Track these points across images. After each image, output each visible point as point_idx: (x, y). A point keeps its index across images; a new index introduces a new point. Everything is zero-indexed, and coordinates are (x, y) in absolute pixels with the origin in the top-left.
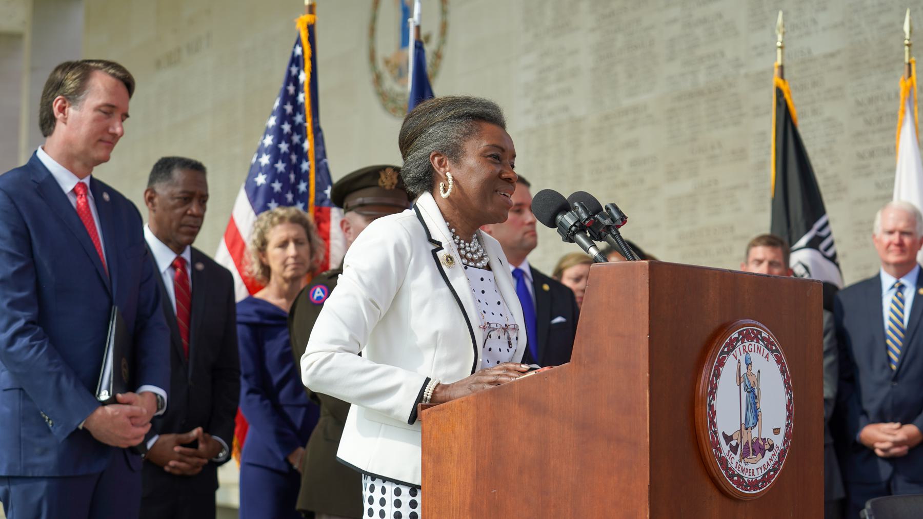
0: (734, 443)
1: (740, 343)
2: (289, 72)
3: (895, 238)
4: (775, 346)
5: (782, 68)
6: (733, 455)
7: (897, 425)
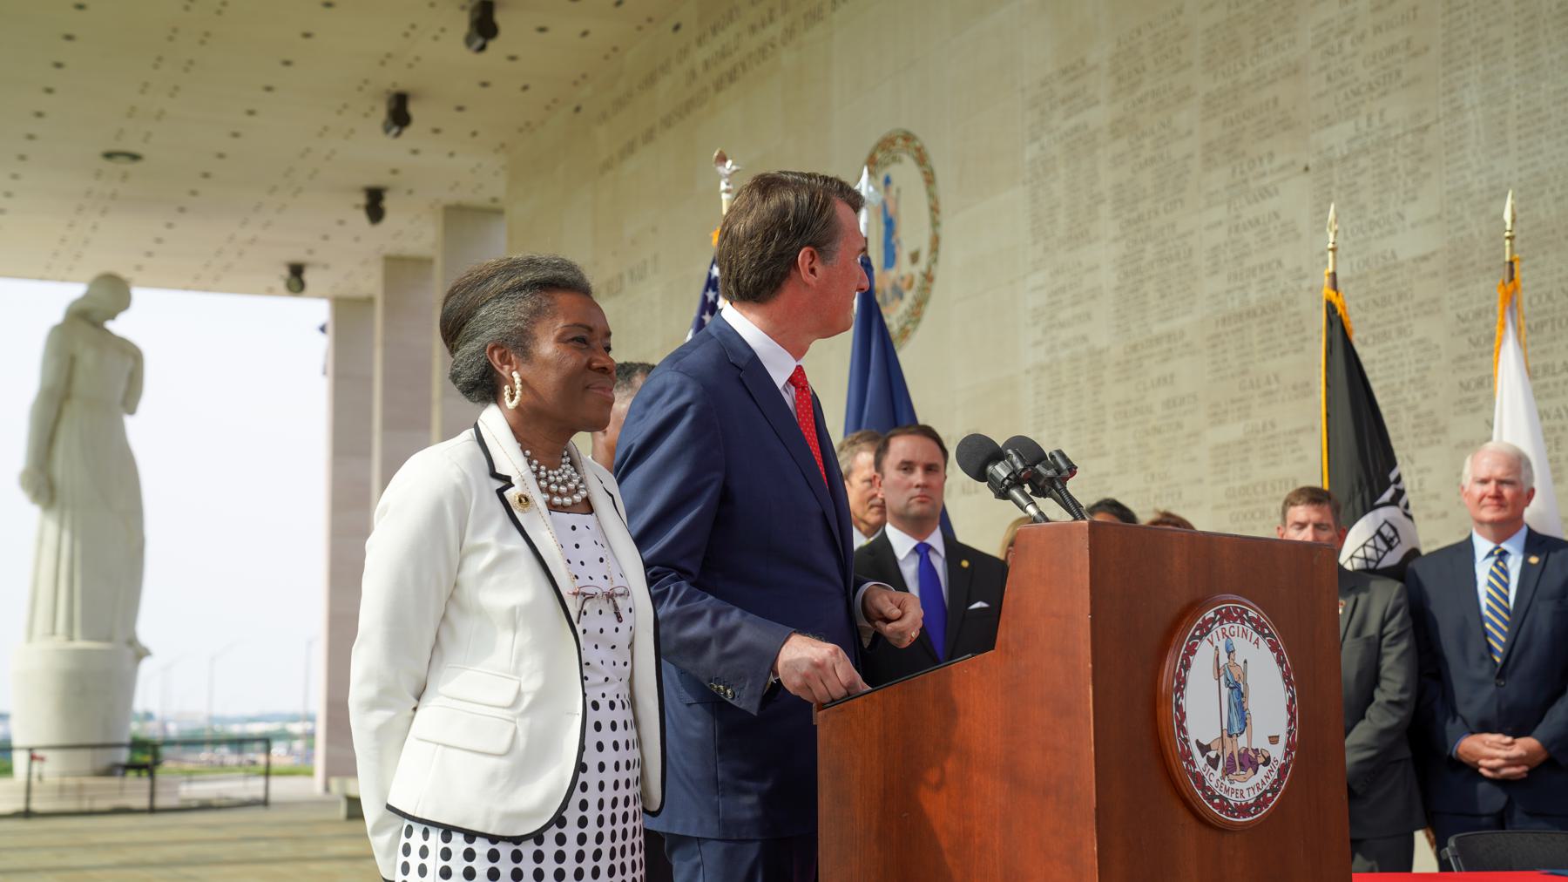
0: (1212, 754)
1: (1217, 624)
2: (705, 298)
3: (1490, 488)
4: (1268, 628)
5: (1334, 275)
6: (1212, 770)
7: (1509, 739)
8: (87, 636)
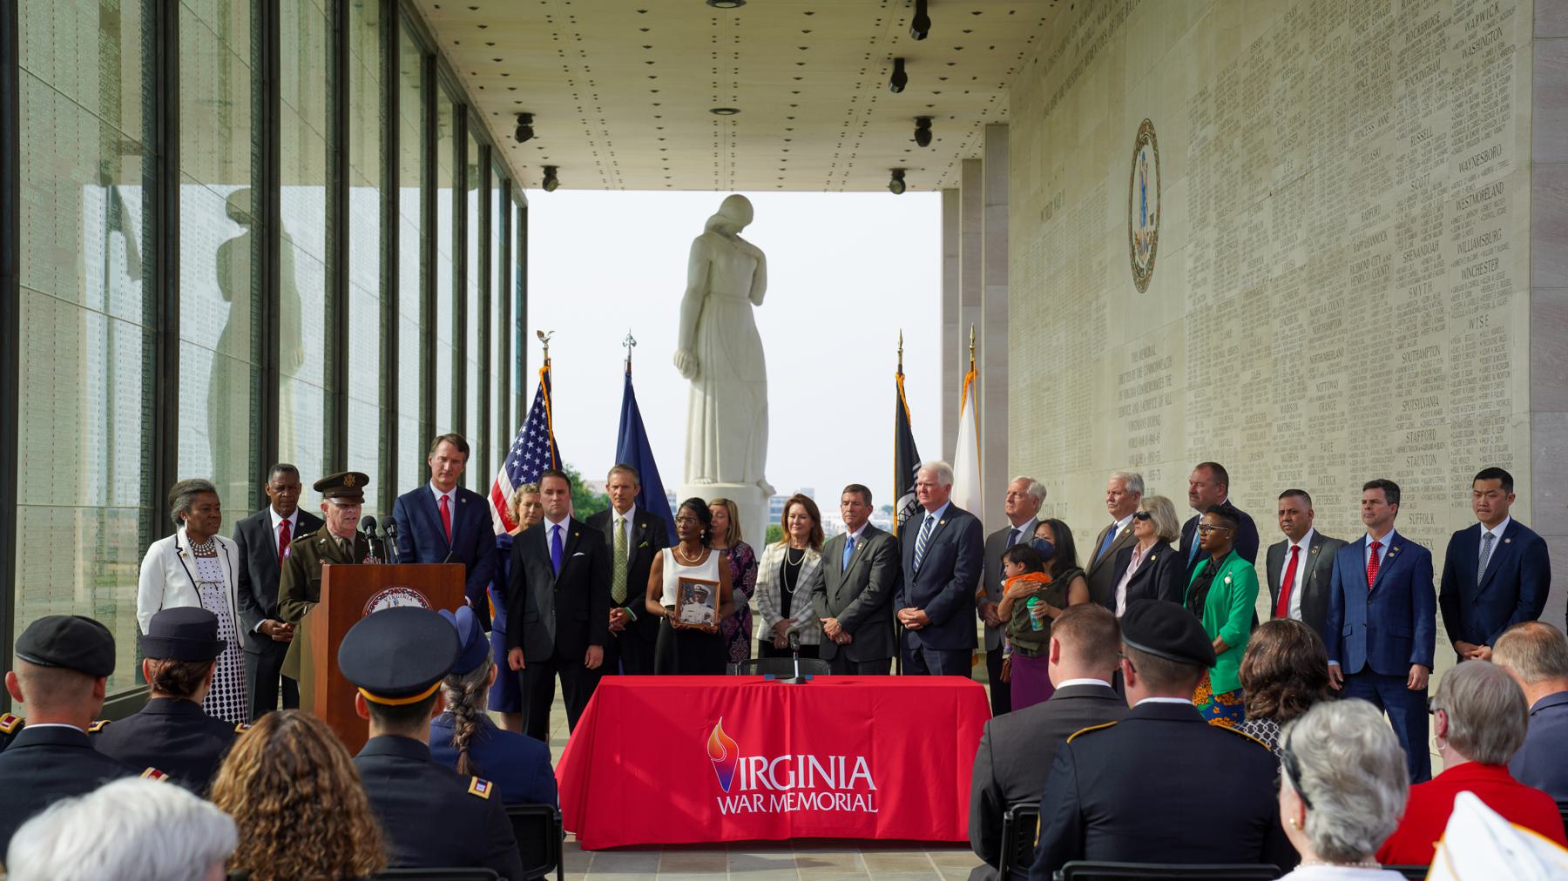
2: (536, 400)
8: (724, 481)
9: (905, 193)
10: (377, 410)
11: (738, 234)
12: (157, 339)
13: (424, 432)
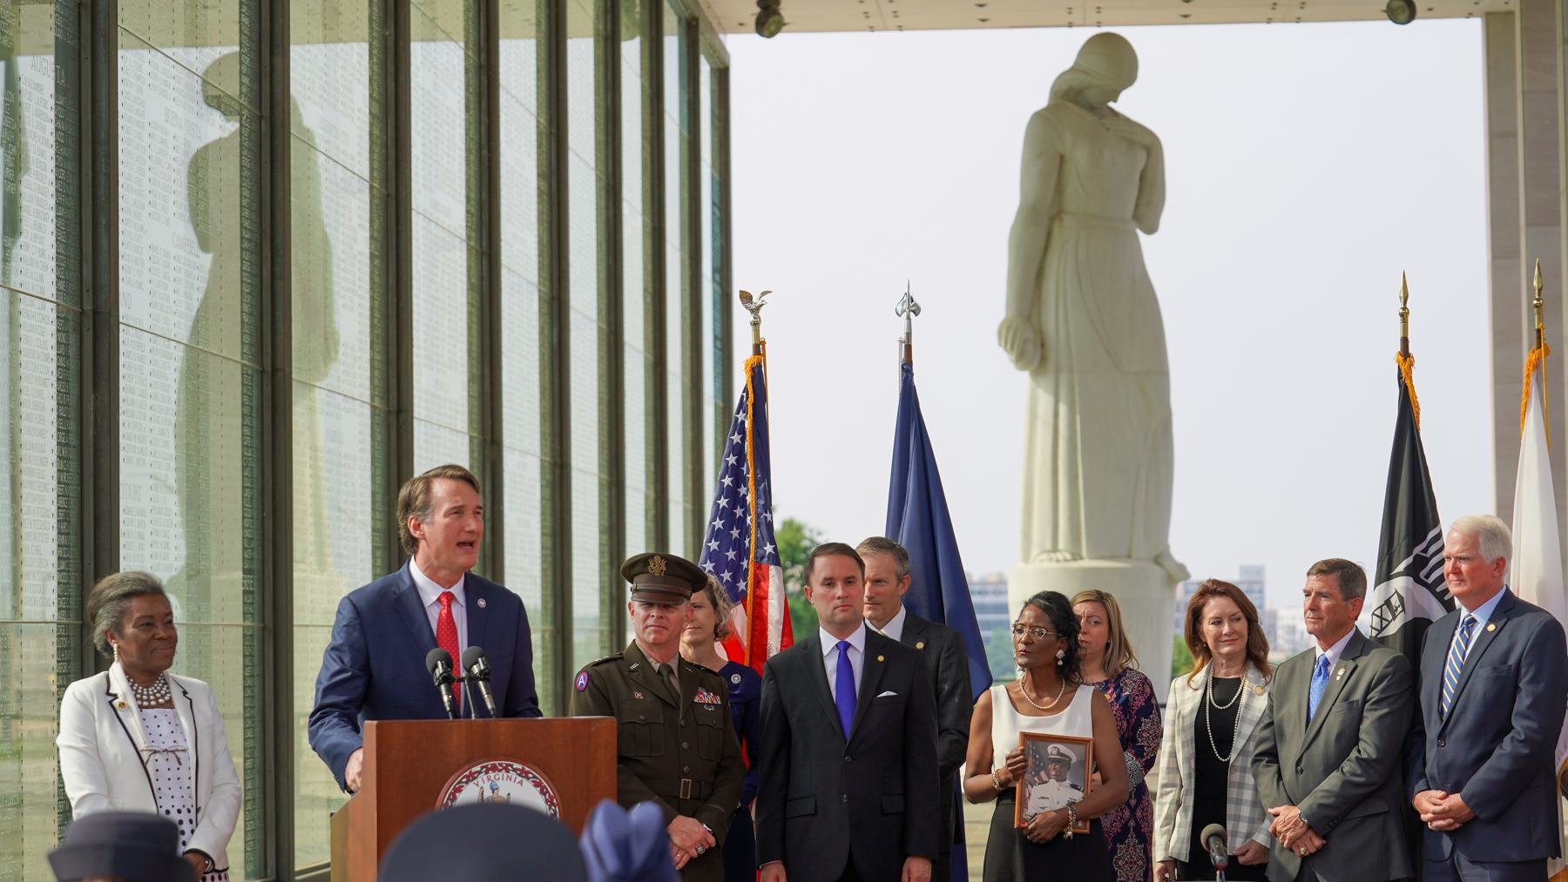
9: (1415, 23)
10: (466, 440)
11: (1111, 104)
12: (81, 325)
13: (548, 477)
